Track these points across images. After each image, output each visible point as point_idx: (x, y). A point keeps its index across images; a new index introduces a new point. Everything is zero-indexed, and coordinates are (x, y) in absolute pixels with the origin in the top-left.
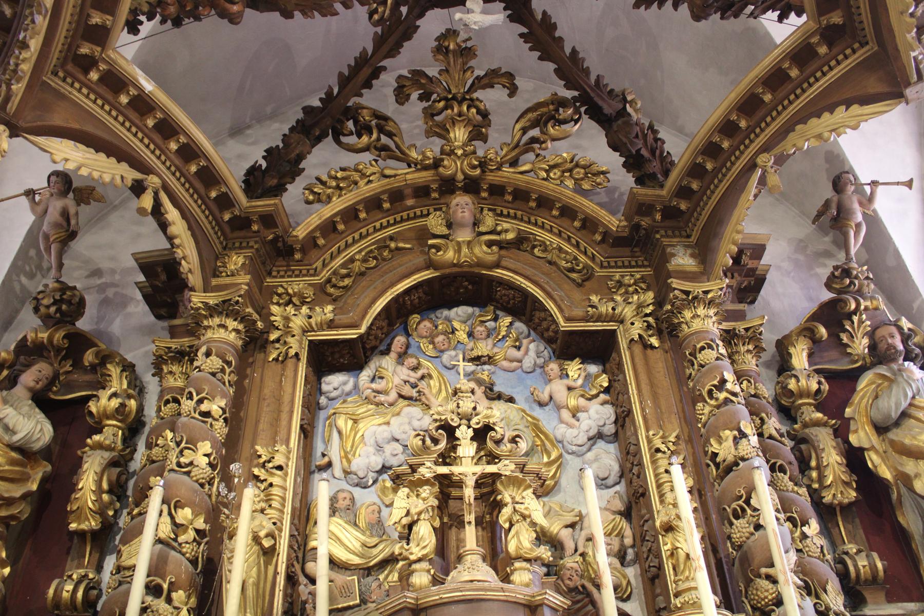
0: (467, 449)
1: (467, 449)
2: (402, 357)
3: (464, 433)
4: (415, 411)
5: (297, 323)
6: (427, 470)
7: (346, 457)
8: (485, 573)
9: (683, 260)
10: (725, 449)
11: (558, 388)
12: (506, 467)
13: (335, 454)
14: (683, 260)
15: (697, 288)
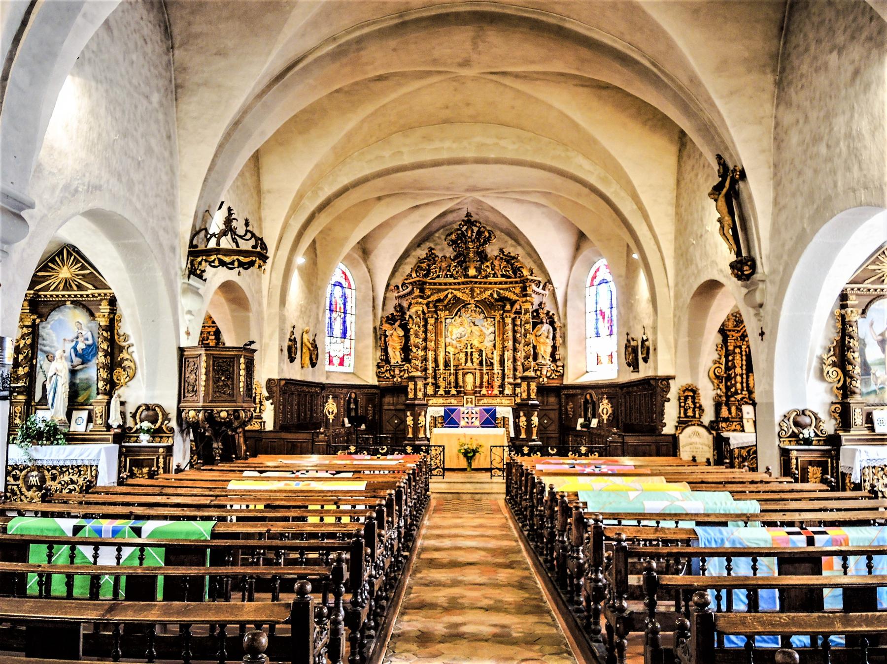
0: (469, 347)
1: (469, 347)
2: (460, 316)
3: (469, 345)
4: (461, 328)
5: (442, 315)
6: (464, 350)
7: (451, 335)
8: (471, 364)
9: (508, 307)
10: (506, 344)
11: (485, 324)
12: (474, 350)
13: (449, 335)
14: (508, 307)
15: (508, 314)
